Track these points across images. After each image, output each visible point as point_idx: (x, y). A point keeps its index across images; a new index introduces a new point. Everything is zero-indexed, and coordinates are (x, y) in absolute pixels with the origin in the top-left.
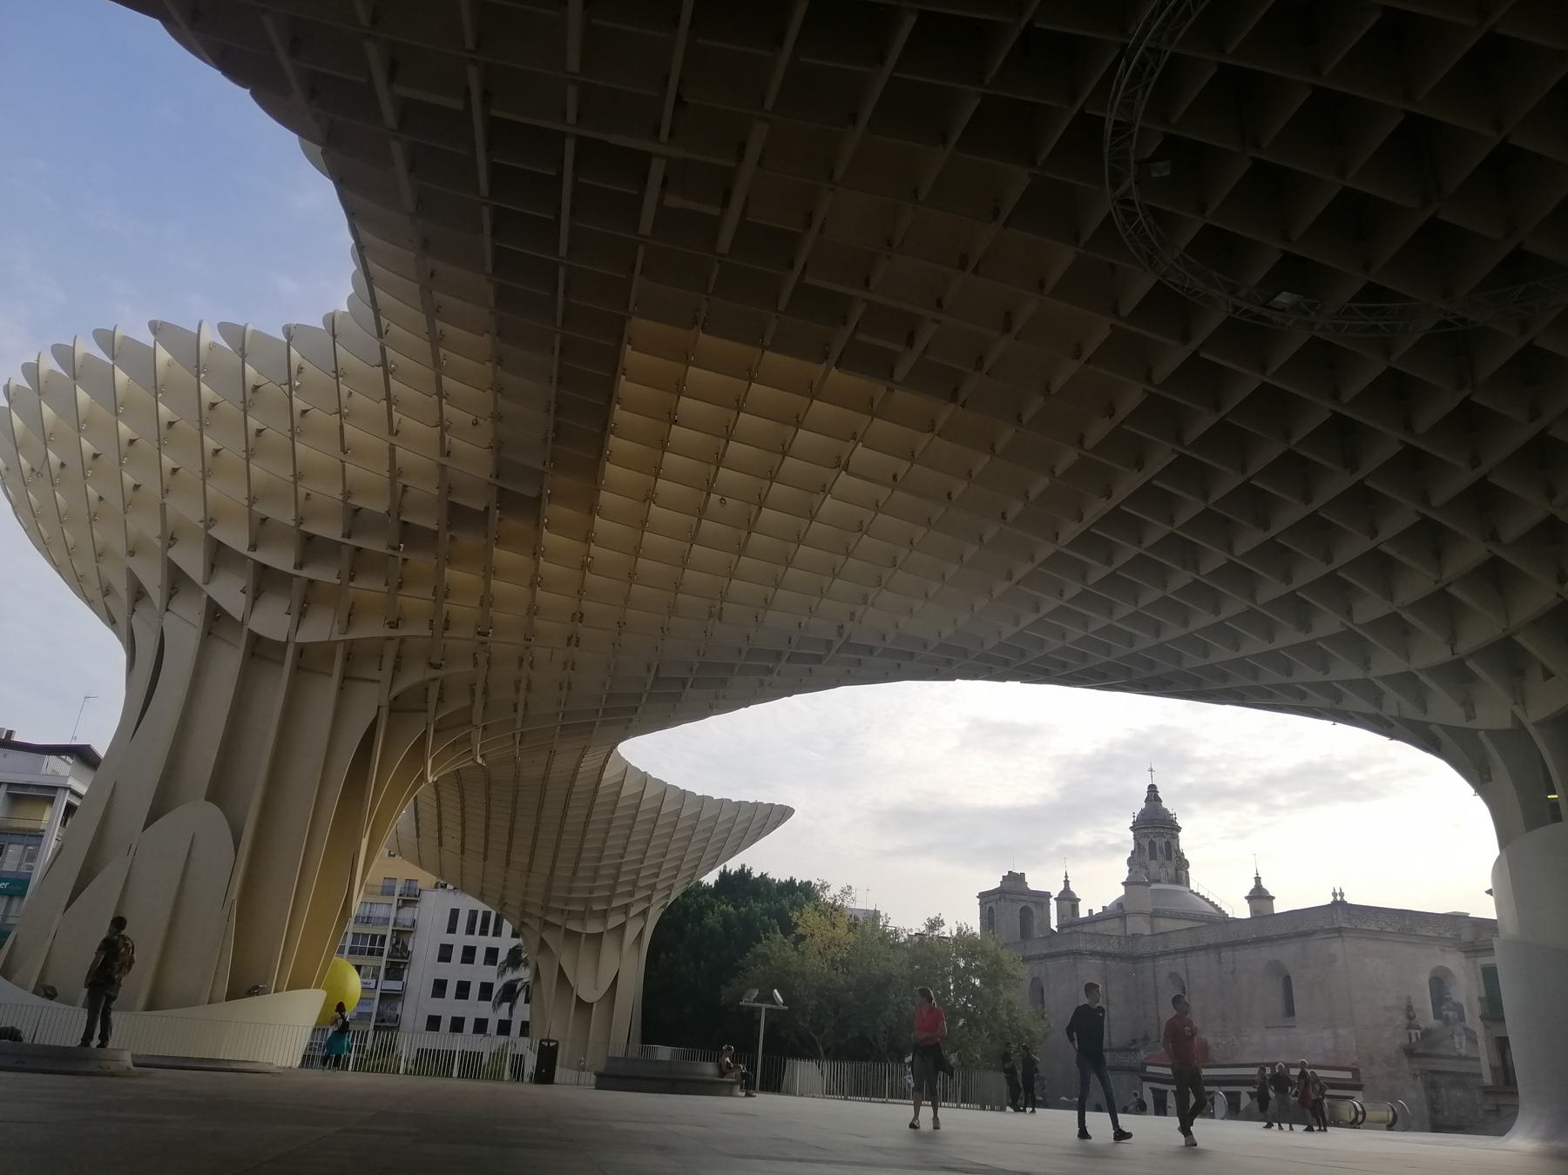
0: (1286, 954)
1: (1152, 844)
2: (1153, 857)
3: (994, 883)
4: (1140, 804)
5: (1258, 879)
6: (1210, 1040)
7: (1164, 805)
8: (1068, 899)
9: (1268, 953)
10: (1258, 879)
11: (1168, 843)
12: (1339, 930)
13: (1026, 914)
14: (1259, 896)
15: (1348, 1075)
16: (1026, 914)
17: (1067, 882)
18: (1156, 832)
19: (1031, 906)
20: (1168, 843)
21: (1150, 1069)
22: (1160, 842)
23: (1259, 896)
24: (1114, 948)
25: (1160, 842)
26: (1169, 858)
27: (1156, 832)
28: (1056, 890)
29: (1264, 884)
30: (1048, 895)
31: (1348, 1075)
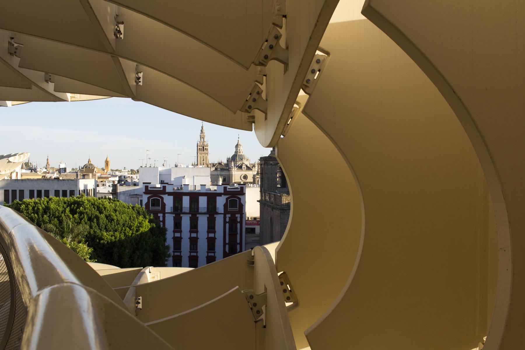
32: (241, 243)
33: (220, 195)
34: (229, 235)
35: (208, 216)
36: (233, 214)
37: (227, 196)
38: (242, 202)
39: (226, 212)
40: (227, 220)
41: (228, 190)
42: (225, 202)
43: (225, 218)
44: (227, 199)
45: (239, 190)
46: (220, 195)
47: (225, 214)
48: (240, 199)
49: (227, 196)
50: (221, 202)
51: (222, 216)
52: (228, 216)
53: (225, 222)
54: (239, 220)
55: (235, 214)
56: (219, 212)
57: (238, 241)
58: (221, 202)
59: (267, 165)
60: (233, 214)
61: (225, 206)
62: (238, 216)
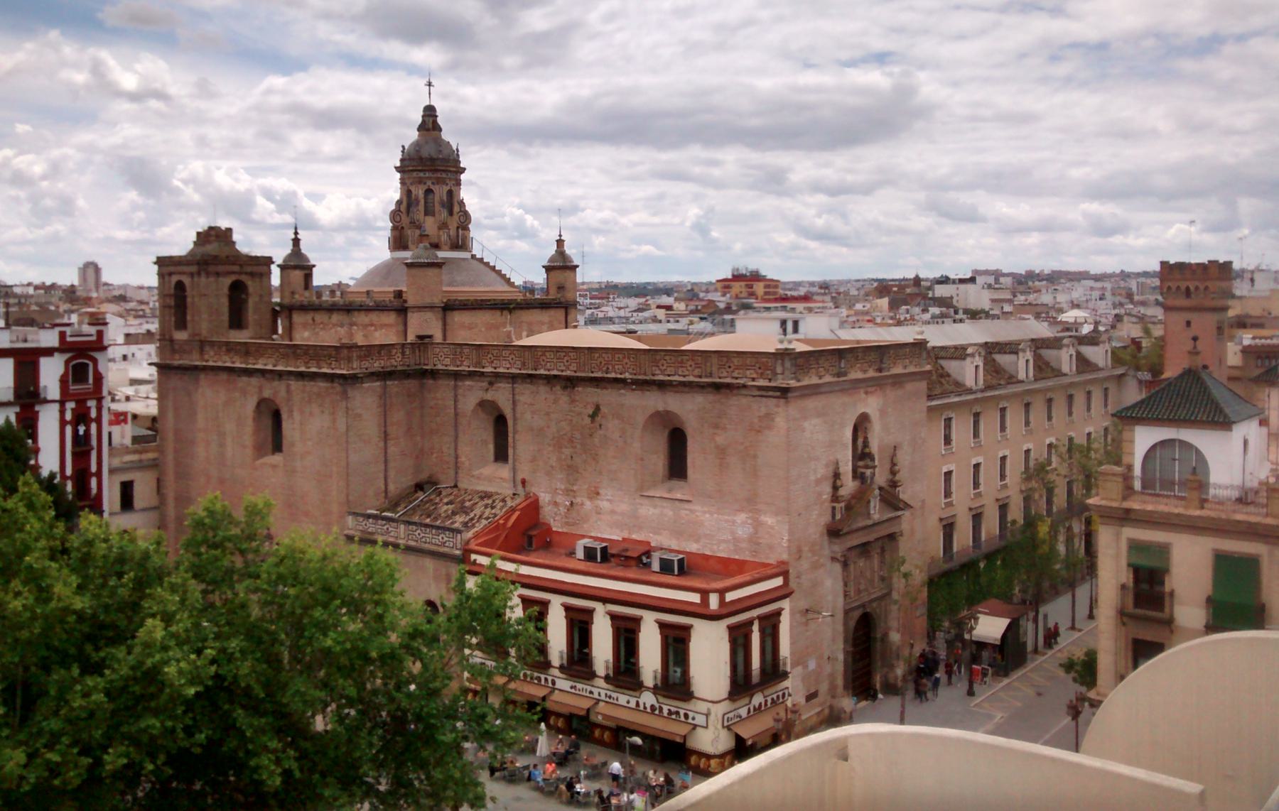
0: (687, 408)
1: (429, 191)
2: (428, 212)
3: (181, 242)
4: (412, 135)
5: (560, 242)
6: (544, 498)
7: (446, 136)
8: (298, 265)
9: (654, 401)
10: (560, 242)
11: (450, 193)
12: (784, 392)
13: (238, 290)
14: (561, 265)
15: (778, 581)
16: (238, 290)
17: (296, 241)
18: (430, 169)
19: (243, 278)
20: (450, 193)
21: (473, 557)
22: (440, 192)
23: (561, 265)
24: (396, 362)
25: (440, 192)
26: (451, 213)
27: (430, 169)
28: (280, 254)
29: (569, 250)
30: (269, 261)
31: (778, 581)
32: (99, 474)
33: (49, 352)
34: (74, 454)
35: (17, 409)
36: (81, 402)
37: (68, 356)
38: (101, 368)
39: (65, 396)
40: (68, 416)
41: (69, 339)
42: (61, 370)
43: (62, 412)
44: (67, 362)
45: (94, 338)
46: (49, 352)
47: (62, 403)
48: (95, 361)
49: (68, 356)
50: (51, 373)
51: (56, 407)
52: (70, 405)
53: (63, 423)
54: (93, 414)
55: (85, 401)
56: (49, 398)
57: (94, 468)
58: (51, 373)
59: (208, 274)
60: (81, 402)
61: (63, 381)
62: (92, 404)
